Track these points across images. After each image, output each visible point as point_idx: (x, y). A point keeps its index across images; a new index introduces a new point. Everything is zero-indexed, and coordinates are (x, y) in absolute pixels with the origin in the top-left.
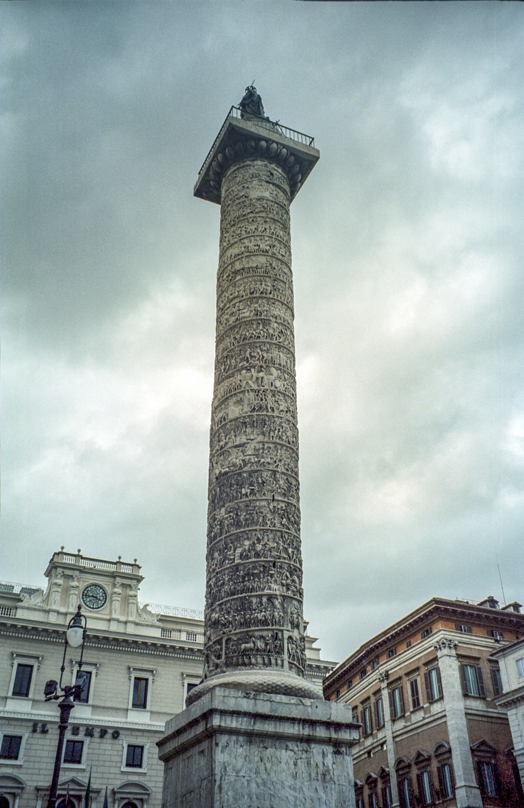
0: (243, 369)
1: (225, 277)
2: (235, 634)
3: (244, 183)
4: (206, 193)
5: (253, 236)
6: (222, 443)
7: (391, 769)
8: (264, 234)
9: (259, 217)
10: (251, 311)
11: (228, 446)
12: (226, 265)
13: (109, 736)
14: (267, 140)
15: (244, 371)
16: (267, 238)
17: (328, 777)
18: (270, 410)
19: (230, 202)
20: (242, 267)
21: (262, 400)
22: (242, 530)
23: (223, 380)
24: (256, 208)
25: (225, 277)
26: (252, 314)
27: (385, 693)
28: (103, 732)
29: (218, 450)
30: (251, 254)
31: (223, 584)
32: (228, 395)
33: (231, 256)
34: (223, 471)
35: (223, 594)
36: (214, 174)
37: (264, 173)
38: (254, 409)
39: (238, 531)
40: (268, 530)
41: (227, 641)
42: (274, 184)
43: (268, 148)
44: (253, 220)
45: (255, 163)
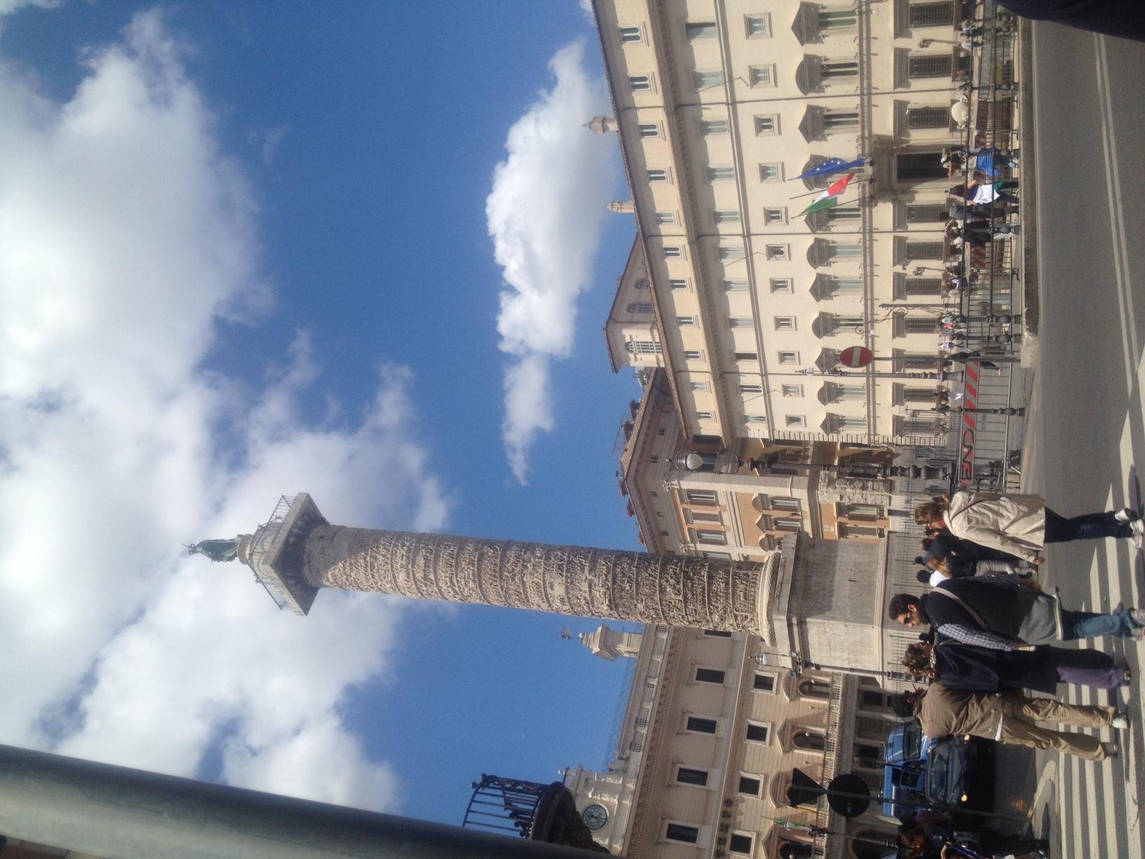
0: (522, 579)
1: (425, 589)
2: (734, 603)
6: (584, 602)
10: (469, 568)
14: (289, 536)
15: (525, 579)
17: (827, 554)
18: (563, 562)
19: (344, 577)
20: (422, 571)
21: (553, 567)
22: (658, 592)
25: (425, 589)
28: (725, 814)
31: (695, 610)
34: (607, 603)
35: (703, 611)
38: (560, 574)
41: (737, 611)
42: (334, 537)
44: (374, 558)
45: (306, 550)
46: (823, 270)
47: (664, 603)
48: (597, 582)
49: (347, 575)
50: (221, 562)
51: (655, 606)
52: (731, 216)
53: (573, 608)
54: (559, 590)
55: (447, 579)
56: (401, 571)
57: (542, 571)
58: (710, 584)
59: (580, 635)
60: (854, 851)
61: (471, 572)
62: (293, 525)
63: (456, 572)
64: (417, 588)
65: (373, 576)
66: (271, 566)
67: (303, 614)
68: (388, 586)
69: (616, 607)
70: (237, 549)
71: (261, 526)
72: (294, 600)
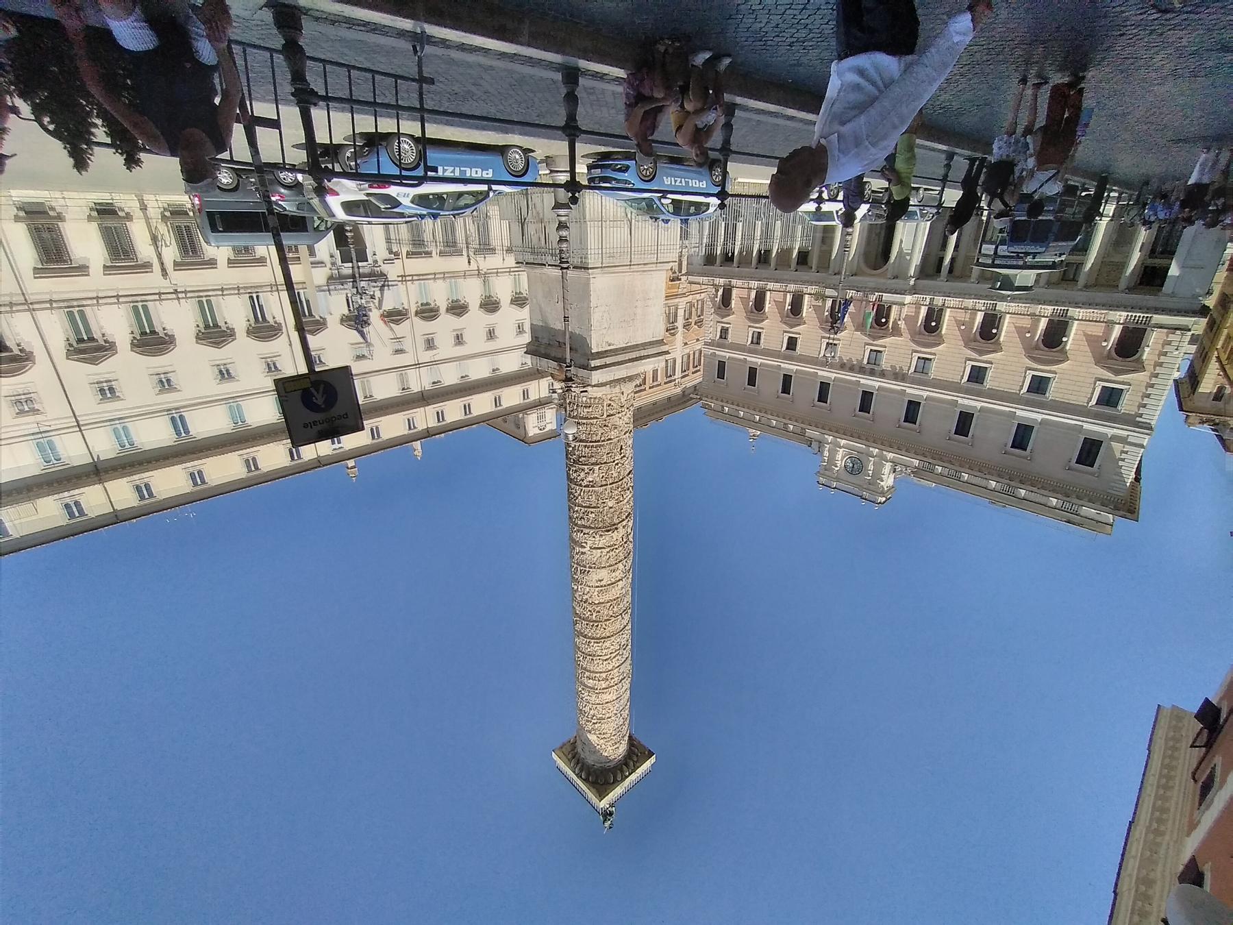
1: (616, 679)
2: (597, 418)
4: (644, 753)
7: (681, 329)
10: (593, 646)
11: (608, 550)
12: (615, 687)
13: (848, 366)
23: (615, 600)
25: (616, 679)
26: (592, 644)
27: (678, 374)
29: (616, 549)
31: (608, 454)
32: (608, 587)
34: (610, 533)
38: (588, 573)
39: (597, 489)
40: (577, 485)
46: (443, 310)
47: (604, 483)
48: (591, 542)
51: (609, 491)
52: (403, 379)
53: (621, 561)
54: (603, 574)
55: (605, 663)
57: (588, 589)
58: (581, 441)
59: (751, 440)
60: (881, 268)
61: (596, 645)
63: (598, 656)
64: (616, 684)
65: (608, 718)
69: (614, 525)
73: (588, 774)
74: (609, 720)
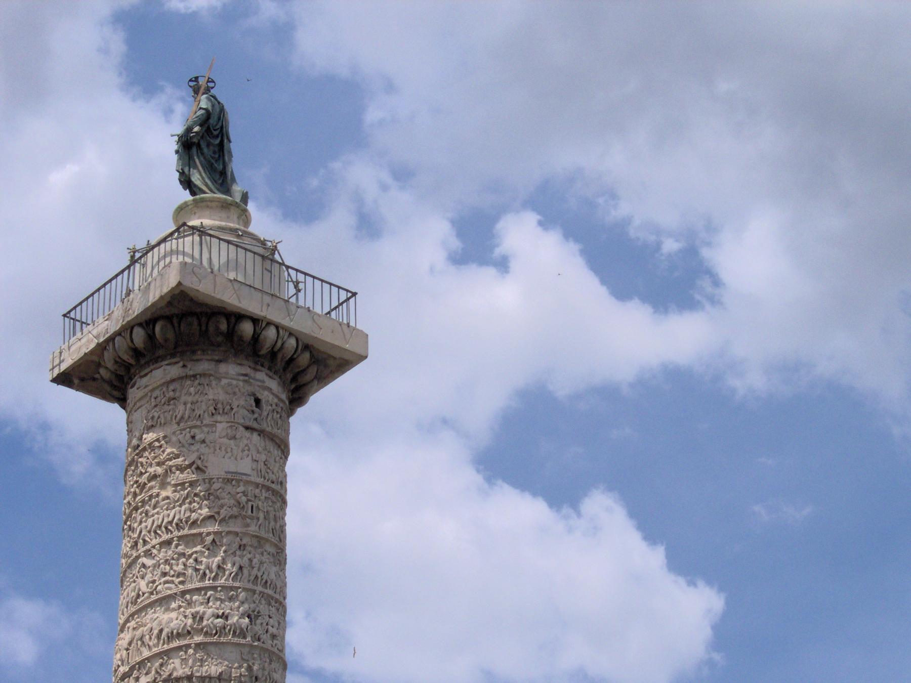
3: (195, 427)
4: (82, 380)
5: (214, 588)
8: (237, 584)
9: (229, 533)
14: (255, 321)
16: (242, 595)
19: (159, 470)
24: (222, 506)
30: (208, 640)
33: (161, 631)
36: (116, 362)
37: (242, 403)
42: (261, 433)
43: (256, 338)
45: (223, 368)
49: (166, 474)
50: (175, 157)
56: (185, 617)
62: (286, 329)
64: (141, 664)
65: (168, 543)
66: (180, 284)
67: (56, 372)
68: (143, 585)
70: (209, 195)
71: (274, 249)
72: (92, 346)
73: (231, 335)
74: (165, 537)
